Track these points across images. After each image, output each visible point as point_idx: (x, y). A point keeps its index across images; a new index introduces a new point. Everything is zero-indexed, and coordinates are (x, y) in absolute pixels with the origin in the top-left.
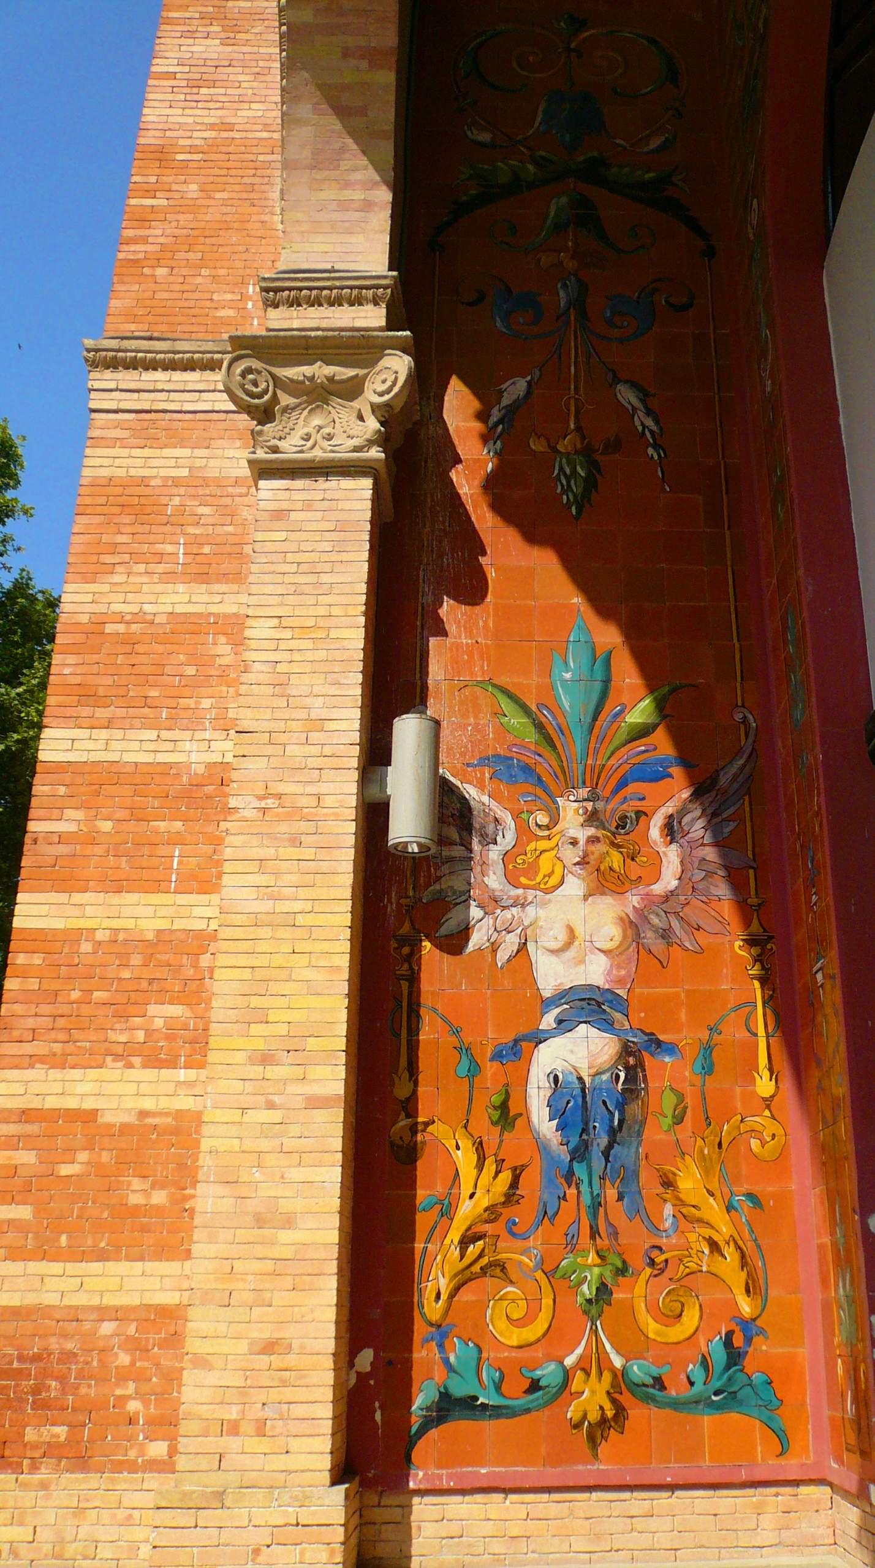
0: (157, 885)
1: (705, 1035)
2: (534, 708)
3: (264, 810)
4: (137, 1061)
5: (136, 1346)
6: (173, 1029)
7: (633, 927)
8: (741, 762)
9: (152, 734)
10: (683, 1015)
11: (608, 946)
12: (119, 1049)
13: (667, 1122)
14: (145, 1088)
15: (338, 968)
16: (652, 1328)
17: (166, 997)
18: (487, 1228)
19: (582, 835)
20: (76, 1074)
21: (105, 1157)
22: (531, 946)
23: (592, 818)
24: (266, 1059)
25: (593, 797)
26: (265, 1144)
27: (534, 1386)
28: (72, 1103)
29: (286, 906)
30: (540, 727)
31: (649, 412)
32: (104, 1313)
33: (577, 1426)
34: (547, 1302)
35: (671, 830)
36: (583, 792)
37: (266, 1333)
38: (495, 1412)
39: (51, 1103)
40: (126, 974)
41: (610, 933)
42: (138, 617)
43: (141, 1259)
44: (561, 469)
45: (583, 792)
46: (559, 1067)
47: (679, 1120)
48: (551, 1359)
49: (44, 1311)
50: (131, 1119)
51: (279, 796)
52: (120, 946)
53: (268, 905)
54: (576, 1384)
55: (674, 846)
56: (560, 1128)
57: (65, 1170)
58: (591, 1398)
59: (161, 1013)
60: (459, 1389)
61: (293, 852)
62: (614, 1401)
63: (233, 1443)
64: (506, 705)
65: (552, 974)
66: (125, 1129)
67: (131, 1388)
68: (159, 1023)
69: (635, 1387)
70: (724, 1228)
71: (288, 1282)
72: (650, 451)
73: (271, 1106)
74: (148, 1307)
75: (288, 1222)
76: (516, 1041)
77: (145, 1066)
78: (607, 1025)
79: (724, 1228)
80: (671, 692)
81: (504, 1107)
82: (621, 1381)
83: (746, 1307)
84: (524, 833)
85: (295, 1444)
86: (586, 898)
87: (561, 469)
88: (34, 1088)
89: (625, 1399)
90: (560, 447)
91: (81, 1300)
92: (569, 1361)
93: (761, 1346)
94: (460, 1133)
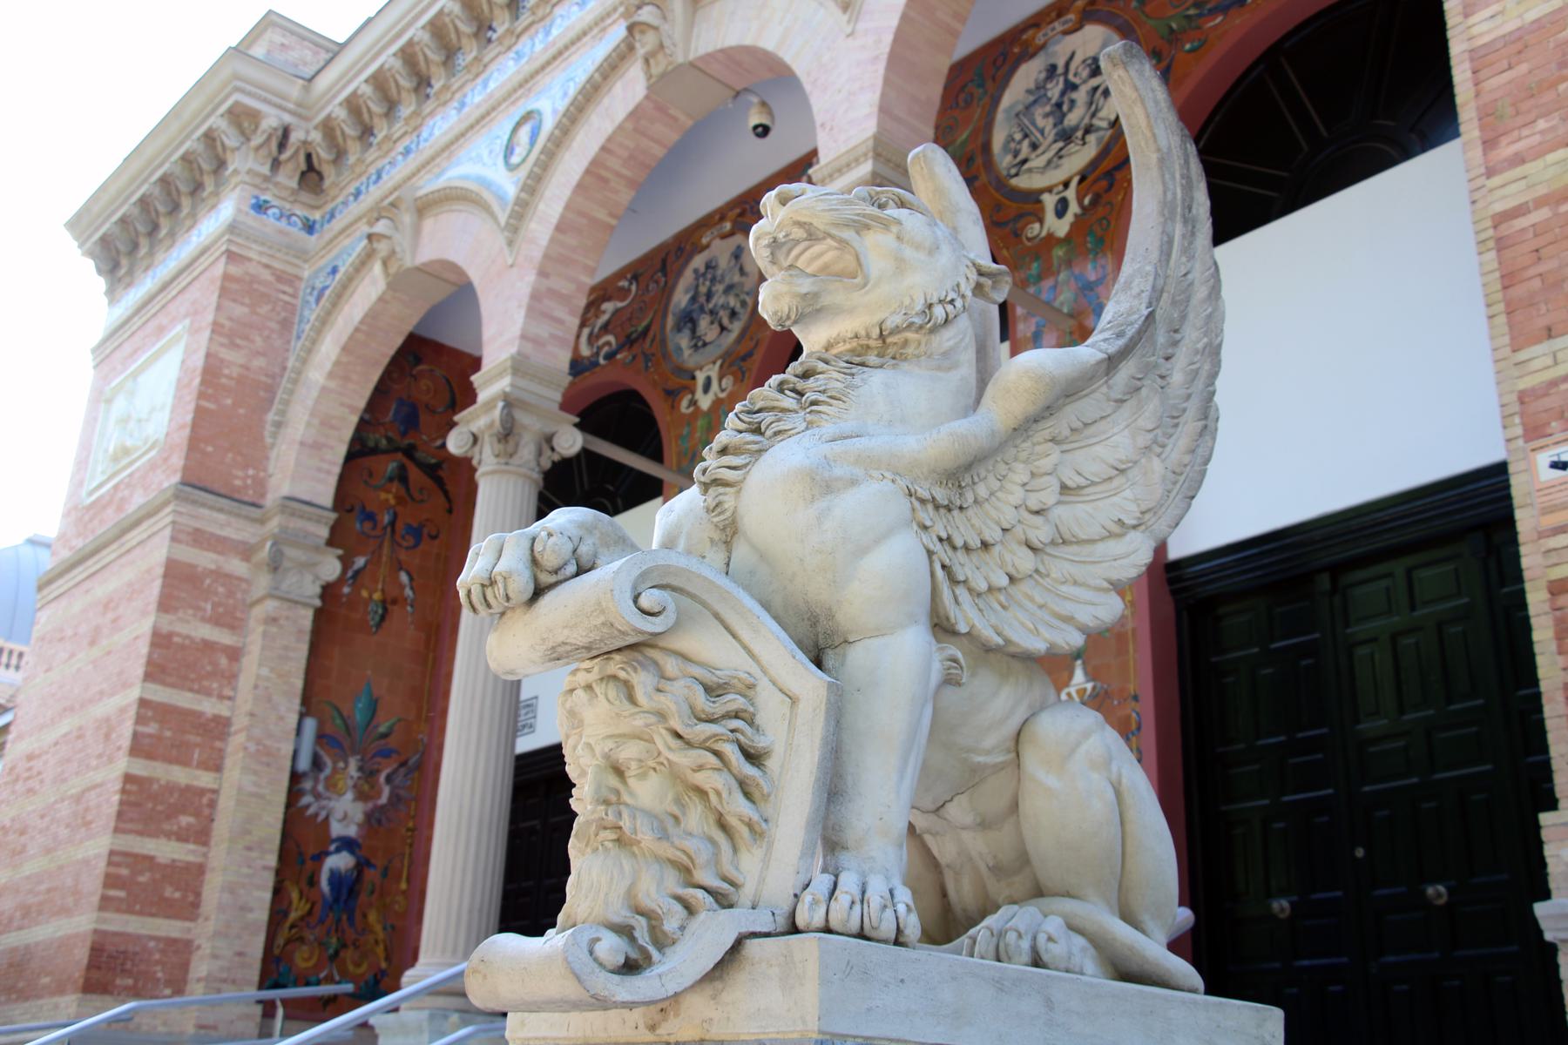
0: (185, 763)
5: (163, 952)
6: (189, 827)
7: (369, 816)
16: (351, 968)
23: (360, 769)
24: (249, 849)
28: (145, 852)
35: (389, 779)
42: (188, 637)
47: (373, 892)
52: (170, 788)
59: (185, 820)
64: (335, 714)
65: (337, 829)
66: (166, 866)
70: (381, 935)
75: (251, 910)
78: (352, 852)
79: (381, 935)
83: (384, 965)
84: (335, 770)
93: (386, 979)
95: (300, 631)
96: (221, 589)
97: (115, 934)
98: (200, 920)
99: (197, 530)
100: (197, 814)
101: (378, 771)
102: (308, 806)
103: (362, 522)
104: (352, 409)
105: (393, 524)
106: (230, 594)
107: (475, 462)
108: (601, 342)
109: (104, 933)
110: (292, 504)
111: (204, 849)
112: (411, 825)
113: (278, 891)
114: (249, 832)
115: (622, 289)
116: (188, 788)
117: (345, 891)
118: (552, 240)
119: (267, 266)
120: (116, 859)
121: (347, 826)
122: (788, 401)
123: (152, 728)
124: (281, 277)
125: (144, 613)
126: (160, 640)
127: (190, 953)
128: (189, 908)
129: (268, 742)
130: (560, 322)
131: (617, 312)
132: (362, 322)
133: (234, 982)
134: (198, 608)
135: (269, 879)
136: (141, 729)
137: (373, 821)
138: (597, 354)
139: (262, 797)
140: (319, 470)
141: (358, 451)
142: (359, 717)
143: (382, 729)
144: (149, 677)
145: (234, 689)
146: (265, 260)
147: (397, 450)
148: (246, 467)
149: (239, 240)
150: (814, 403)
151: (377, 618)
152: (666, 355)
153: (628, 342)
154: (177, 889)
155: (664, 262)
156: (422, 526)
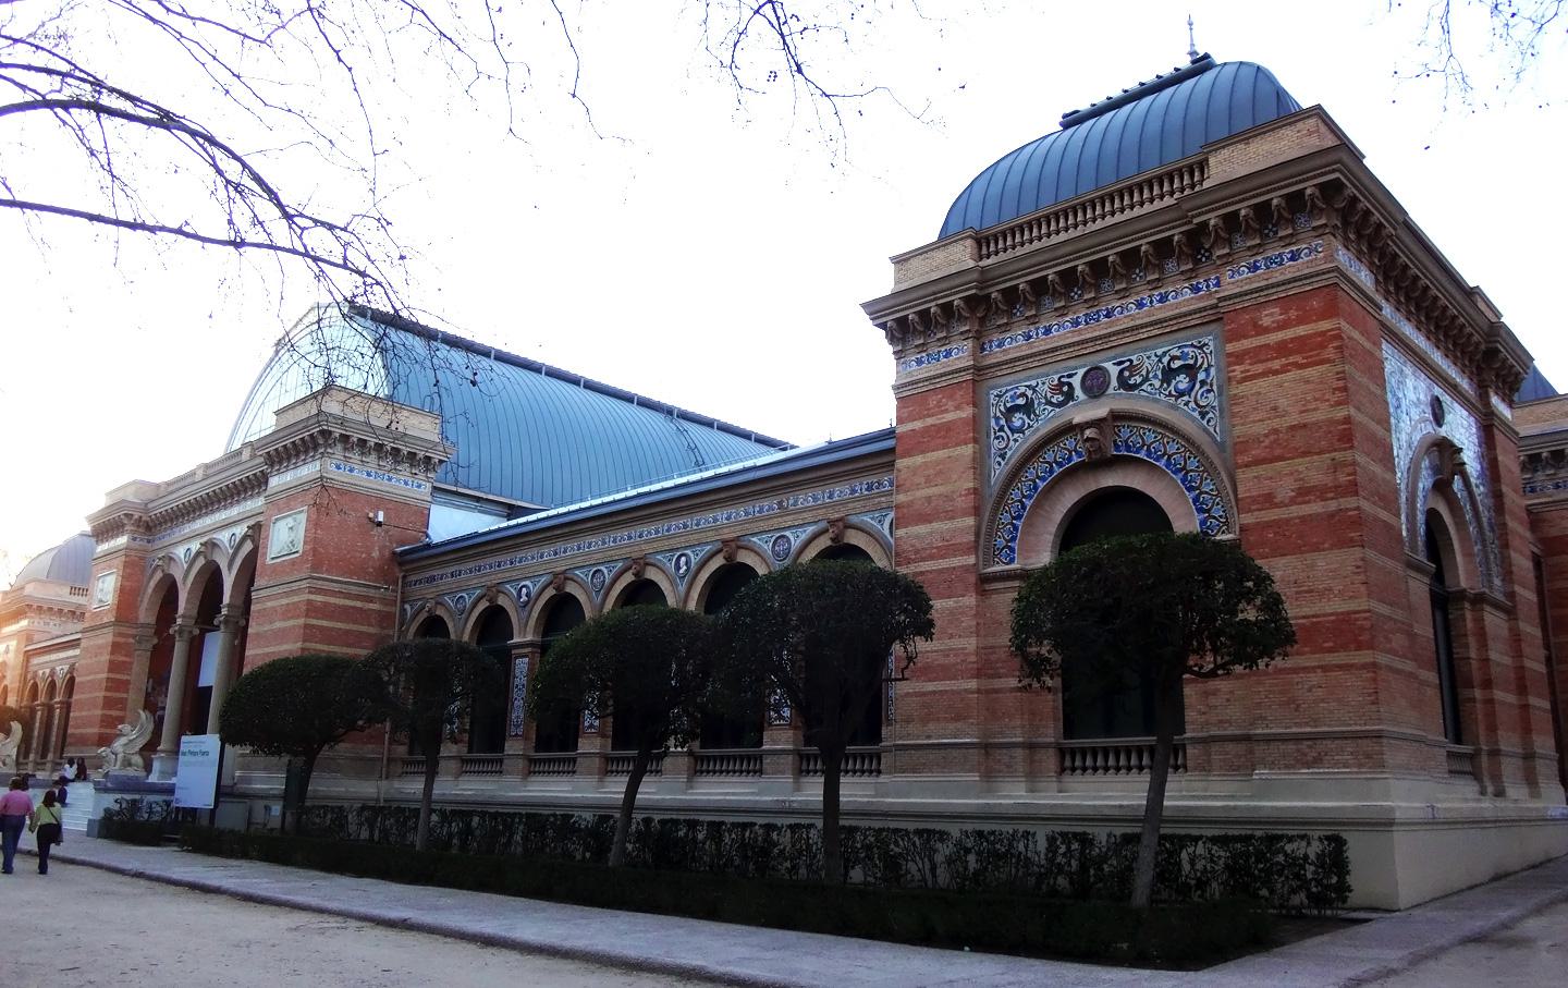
110: (143, 626)
123: (110, 684)
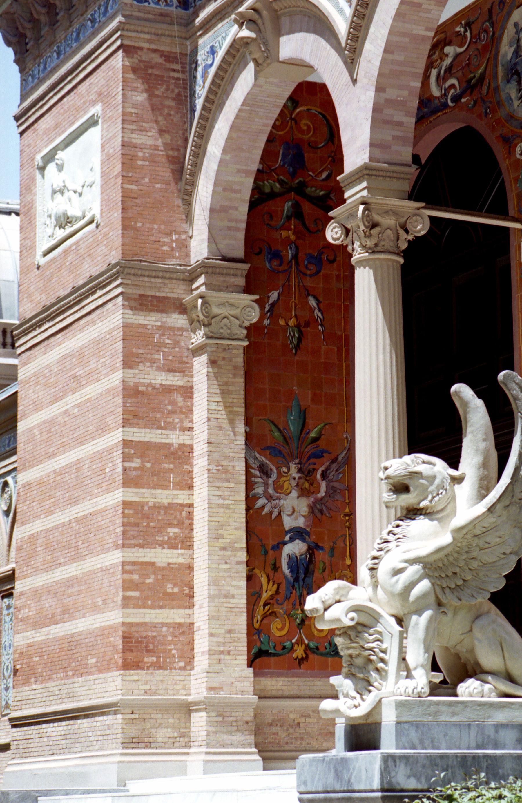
0: (165, 487)
1: (332, 544)
2: (282, 429)
3: (218, 470)
4: (166, 546)
7: (312, 508)
8: (345, 452)
9: (159, 431)
10: (326, 538)
11: (304, 514)
12: (159, 542)
13: (321, 571)
14: (169, 556)
15: (242, 523)
17: (171, 525)
18: (271, 601)
19: (297, 476)
20: (148, 550)
21: (159, 577)
22: (282, 513)
23: (300, 470)
24: (224, 549)
25: (300, 463)
26: (226, 574)
27: (284, 648)
28: (147, 560)
29: (227, 502)
30: (283, 435)
31: (320, 310)
32: (163, 624)
33: (296, 659)
34: (287, 624)
35: (324, 476)
36: (297, 461)
37: (229, 628)
38: (274, 655)
39: (141, 560)
40: (160, 518)
41: (304, 510)
42: (150, 385)
43: (173, 608)
44: (290, 333)
45: (297, 461)
46: (290, 552)
47: (324, 570)
48: (288, 640)
49: (146, 624)
50: (166, 565)
51: (222, 466)
52: (157, 507)
53: (221, 502)
54: (296, 647)
55: (324, 481)
56: (291, 572)
57: (148, 581)
58: (299, 652)
59: (173, 531)
60: (264, 648)
61: (226, 485)
62: (305, 653)
63: (222, 656)
64: (273, 428)
65: (288, 522)
66: (164, 569)
67: (172, 647)
68: (171, 534)
69: (311, 649)
71: (234, 614)
72: (320, 327)
73: (226, 563)
74: (176, 623)
75: (233, 597)
76: (278, 544)
77: (169, 548)
78: (303, 540)
80: (325, 425)
81: (275, 565)
82: (307, 648)
84: (280, 475)
85: (238, 657)
86: (298, 497)
87: (290, 333)
88: (136, 555)
89: (308, 652)
90: (289, 324)
91: (157, 621)
92: (294, 641)
94: (262, 572)
95: (235, 368)
96: (168, 341)
97: (137, 624)
98: (195, 607)
99: (141, 296)
100: (180, 524)
101: (315, 470)
102: (263, 507)
103: (269, 262)
104: (247, 173)
105: (295, 257)
106: (176, 343)
107: (349, 248)
108: (447, 84)
109: (131, 624)
111: (190, 552)
112: (347, 510)
113: (250, 578)
114: (221, 536)
115: (458, 34)
116: (170, 506)
117: (302, 571)
118: (383, 61)
119: (155, 51)
120: (127, 568)
121: (296, 519)
122: (391, 538)
123: (136, 463)
124: (169, 57)
125: (114, 370)
126: (131, 392)
127: (193, 633)
128: (187, 599)
129: (224, 463)
130: (400, 124)
131: (457, 56)
132: (243, 104)
133: (229, 653)
134: (153, 361)
135: (243, 570)
136: (127, 464)
137: (316, 512)
138: (445, 95)
139: (228, 507)
140: (229, 228)
141: (259, 200)
142: (293, 428)
143: (313, 435)
144: (126, 422)
145: (192, 421)
146: (153, 46)
147: (290, 190)
148: (170, 234)
149: (130, 34)
150: (399, 538)
151: (295, 342)
152: (499, 103)
153: (470, 87)
154: (175, 585)
155: (490, 11)
156: (320, 253)
